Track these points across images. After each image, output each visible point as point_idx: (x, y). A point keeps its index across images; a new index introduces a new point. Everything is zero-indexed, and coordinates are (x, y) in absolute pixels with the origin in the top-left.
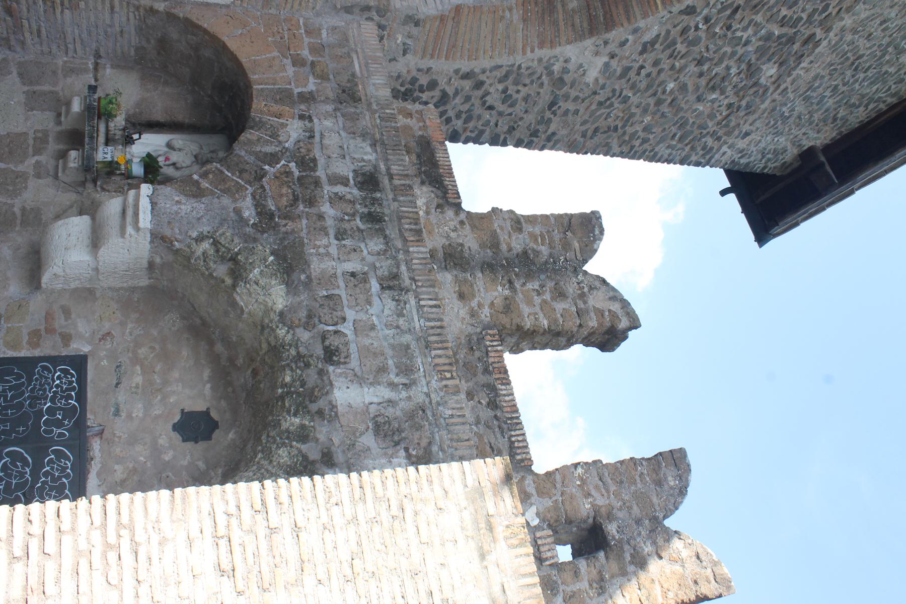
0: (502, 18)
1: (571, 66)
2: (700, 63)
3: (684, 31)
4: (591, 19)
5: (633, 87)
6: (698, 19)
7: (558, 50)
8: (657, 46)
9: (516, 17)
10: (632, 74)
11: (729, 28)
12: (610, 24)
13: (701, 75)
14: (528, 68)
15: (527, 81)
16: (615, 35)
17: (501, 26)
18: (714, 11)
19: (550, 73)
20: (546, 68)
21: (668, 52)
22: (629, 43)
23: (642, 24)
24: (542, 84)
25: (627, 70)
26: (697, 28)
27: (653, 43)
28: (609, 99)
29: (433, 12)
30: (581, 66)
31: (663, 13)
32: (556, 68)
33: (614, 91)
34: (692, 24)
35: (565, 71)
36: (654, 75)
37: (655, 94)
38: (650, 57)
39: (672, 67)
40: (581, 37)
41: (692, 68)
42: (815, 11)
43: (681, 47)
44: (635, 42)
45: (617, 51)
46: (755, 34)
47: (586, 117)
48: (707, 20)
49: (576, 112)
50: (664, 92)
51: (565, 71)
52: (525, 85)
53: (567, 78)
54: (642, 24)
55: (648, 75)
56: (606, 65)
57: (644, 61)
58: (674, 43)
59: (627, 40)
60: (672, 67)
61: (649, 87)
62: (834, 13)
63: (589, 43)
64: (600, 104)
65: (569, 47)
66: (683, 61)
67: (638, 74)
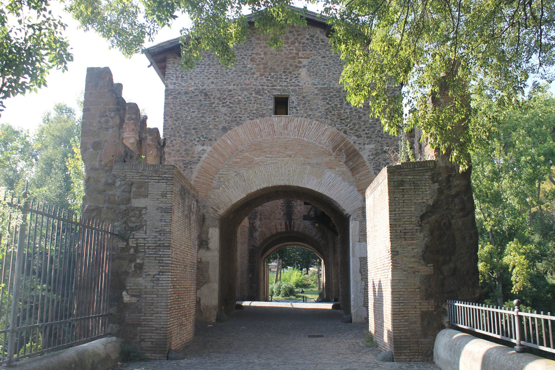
0: (359, 179)
1: (370, 153)
2: (360, 118)
3: (351, 129)
4: (354, 156)
5: (374, 132)
6: (347, 128)
7: (366, 160)
8: (358, 134)
9: (358, 176)
10: (369, 135)
11: (347, 118)
12: (355, 150)
13: (365, 114)
14: (374, 165)
15: (378, 163)
16: (357, 147)
17: (361, 178)
18: (343, 125)
19: (374, 158)
20: (372, 160)
21: (359, 130)
22: (359, 142)
23: (352, 142)
24: (379, 158)
25: (368, 137)
26: (350, 126)
27: (357, 136)
28: (380, 136)
29: (361, 196)
30: (370, 151)
31: (347, 139)
32: (372, 157)
33: (376, 137)
34: (349, 128)
35: (372, 154)
36: (368, 129)
37: (375, 124)
38: (362, 133)
39: (364, 124)
40: (361, 156)
41: (363, 119)
42: (336, 97)
43: (357, 127)
44: (358, 141)
45: (362, 144)
46: (348, 108)
47: (388, 139)
48: (347, 125)
49: (387, 143)
50: (373, 121)
51: (372, 154)
52: (380, 163)
53: (374, 152)
54: (352, 142)
55: (368, 130)
56: (367, 144)
57: (364, 134)
58: (356, 130)
59: (358, 143)
60: (364, 124)
61: (372, 127)
62: (335, 91)
63: (361, 153)
64: (382, 138)
65: (364, 157)
66: (361, 123)
67: (369, 133)
